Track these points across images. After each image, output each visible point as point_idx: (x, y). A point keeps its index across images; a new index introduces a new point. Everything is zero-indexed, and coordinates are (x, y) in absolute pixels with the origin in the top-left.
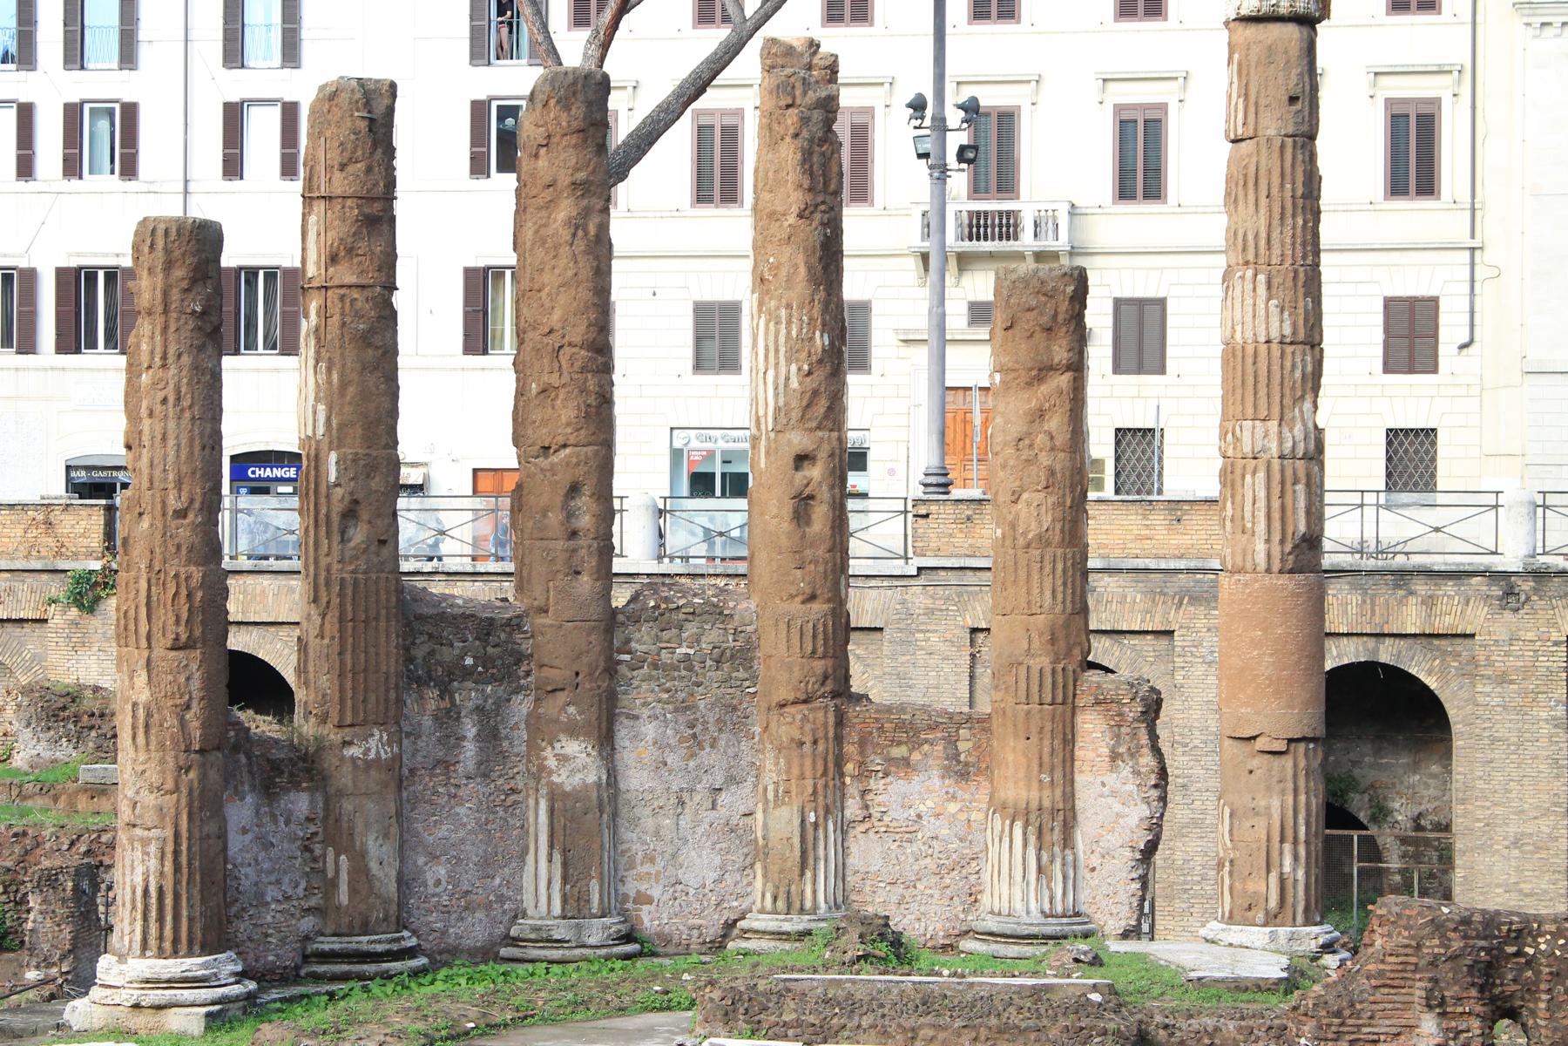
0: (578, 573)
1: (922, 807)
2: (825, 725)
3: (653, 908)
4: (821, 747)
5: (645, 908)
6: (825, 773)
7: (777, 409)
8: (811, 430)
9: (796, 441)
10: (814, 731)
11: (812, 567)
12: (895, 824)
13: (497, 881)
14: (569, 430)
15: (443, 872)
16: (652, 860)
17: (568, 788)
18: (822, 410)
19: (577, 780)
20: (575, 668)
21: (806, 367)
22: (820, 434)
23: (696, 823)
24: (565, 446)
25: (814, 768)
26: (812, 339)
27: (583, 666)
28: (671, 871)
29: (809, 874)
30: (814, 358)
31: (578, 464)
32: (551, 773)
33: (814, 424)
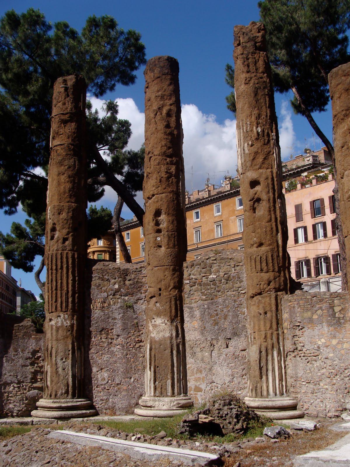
0: (161, 247)
1: (320, 343)
2: (270, 304)
3: (202, 393)
4: (269, 315)
5: (199, 393)
6: (271, 327)
7: (242, 164)
8: (256, 170)
9: (249, 176)
10: (264, 308)
11: (259, 230)
12: (308, 352)
13: (132, 380)
14: (154, 188)
15: (106, 375)
16: (201, 372)
17: (157, 339)
18: (261, 160)
19: (161, 335)
20: (159, 287)
21: (250, 143)
22: (261, 171)
23: (220, 355)
24: (153, 195)
25: (265, 325)
26: (252, 131)
27: (162, 285)
28: (209, 376)
29: (264, 378)
30: (253, 138)
31: (157, 202)
32: (151, 332)
33: (258, 167)
